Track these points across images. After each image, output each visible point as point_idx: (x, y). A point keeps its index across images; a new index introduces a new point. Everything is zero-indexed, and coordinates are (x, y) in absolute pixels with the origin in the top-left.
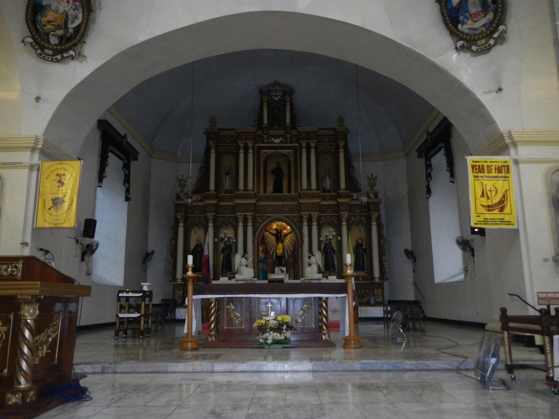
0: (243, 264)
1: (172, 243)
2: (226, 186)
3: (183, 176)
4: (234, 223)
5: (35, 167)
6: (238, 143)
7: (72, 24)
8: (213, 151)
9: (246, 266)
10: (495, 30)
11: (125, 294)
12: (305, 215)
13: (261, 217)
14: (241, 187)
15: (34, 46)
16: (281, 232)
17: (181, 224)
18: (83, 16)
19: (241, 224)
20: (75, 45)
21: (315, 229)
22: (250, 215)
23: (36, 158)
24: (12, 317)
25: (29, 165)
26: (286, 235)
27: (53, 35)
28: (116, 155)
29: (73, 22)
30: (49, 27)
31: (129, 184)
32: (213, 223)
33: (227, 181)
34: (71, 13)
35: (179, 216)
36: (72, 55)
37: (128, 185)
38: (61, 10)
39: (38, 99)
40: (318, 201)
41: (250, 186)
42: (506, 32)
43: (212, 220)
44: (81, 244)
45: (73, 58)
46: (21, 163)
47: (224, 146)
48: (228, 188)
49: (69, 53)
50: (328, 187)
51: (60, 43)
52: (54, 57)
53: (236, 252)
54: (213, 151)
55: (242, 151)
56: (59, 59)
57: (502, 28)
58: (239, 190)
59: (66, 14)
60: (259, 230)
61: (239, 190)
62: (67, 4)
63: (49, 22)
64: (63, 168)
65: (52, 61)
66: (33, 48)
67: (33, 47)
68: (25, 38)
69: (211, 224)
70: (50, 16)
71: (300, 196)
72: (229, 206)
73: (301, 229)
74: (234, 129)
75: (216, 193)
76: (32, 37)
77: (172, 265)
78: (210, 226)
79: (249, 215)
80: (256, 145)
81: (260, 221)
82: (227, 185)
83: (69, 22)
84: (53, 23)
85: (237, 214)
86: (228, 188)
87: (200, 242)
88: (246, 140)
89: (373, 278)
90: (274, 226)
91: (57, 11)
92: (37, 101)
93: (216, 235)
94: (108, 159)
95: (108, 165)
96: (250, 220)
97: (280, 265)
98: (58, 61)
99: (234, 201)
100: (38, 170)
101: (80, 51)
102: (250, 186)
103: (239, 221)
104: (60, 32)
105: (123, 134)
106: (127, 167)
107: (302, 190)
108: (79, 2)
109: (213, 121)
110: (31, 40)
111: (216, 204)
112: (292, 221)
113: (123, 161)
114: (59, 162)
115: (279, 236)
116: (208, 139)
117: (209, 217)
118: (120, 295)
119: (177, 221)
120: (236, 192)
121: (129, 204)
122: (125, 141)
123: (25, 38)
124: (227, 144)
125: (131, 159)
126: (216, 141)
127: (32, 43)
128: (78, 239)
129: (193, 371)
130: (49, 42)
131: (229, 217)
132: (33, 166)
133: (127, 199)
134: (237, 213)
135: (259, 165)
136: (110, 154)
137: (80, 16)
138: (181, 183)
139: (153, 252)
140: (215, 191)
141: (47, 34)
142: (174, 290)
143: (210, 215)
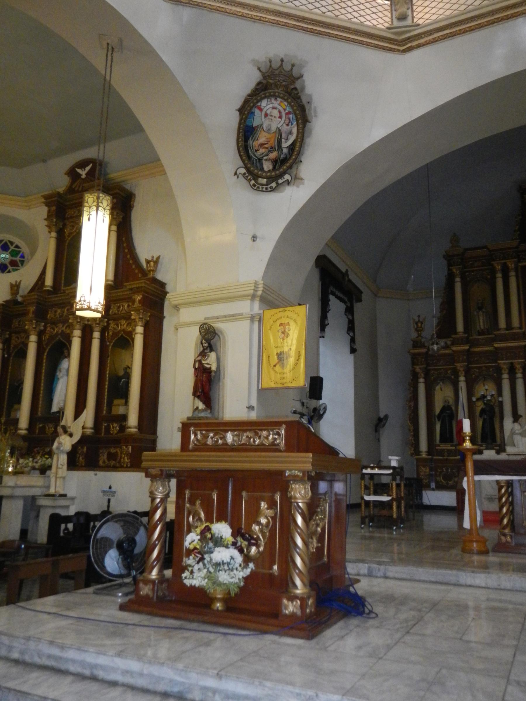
0: (517, 432)
1: (411, 405)
2: (480, 325)
3: (419, 316)
4: (495, 375)
5: (256, 317)
6: (492, 265)
7: (286, 142)
8: (458, 279)
11: (369, 471)
14: (502, 324)
15: (247, 177)
17: (421, 380)
18: (298, 130)
19: (505, 376)
20: (290, 167)
22: (519, 363)
24: (278, 497)
25: (250, 316)
27: (266, 160)
28: (337, 297)
31: (354, 332)
32: (465, 376)
33: (481, 318)
34: (285, 129)
35: (418, 369)
36: (288, 180)
37: (353, 334)
38: (274, 129)
39: (254, 238)
41: (516, 322)
43: (463, 372)
44: (307, 408)
45: (288, 183)
46: (241, 314)
47: (473, 271)
48: (482, 327)
49: (284, 178)
51: (274, 168)
52: (269, 186)
54: (458, 279)
55: (499, 275)
56: (274, 187)
58: (499, 330)
59: (279, 130)
61: (499, 330)
62: (280, 120)
63: (262, 145)
64: (286, 316)
65: (267, 190)
66: (246, 179)
67: (246, 178)
68: (238, 169)
69: (462, 378)
72: (486, 352)
74: (486, 247)
75: (466, 335)
76: (244, 166)
77: (412, 434)
78: (461, 381)
79: (518, 362)
80: (520, 264)
82: (482, 324)
83: (283, 140)
84: (266, 146)
85: (499, 364)
86: (482, 327)
87: (449, 402)
91: (269, 131)
92: (254, 241)
93: (470, 393)
94: (330, 303)
95: (330, 310)
96: (519, 370)
98: (273, 190)
99: (493, 345)
100: (260, 321)
101: (296, 174)
102: (516, 322)
103: (503, 371)
105: (344, 271)
106: (349, 311)
108: (293, 113)
109: (455, 240)
110: (243, 171)
111: (468, 350)
113: (345, 304)
114: (281, 309)
116: (449, 265)
117: (458, 368)
118: (364, 471)
119: (415, 376)
120: (496, 333)
121: (355, 357)
122: (347, 279)
123: (238, 169)
124: (478, 268)
125: (354, 301)
126: (461, 266)
127: (245, 174)
128: (304, 401)
129: (499, 587)
130: (262, 169)
131: (488, 368)
132: (254, 316)
133: (353, 351)
134: (499, 362)
136: (331, 297)
137: (295, 130)
138: (417, 325)
139: (386, 417)
140: (465, 332)
141: (260, 160)
142: (418, 466)
143: (460, 366)
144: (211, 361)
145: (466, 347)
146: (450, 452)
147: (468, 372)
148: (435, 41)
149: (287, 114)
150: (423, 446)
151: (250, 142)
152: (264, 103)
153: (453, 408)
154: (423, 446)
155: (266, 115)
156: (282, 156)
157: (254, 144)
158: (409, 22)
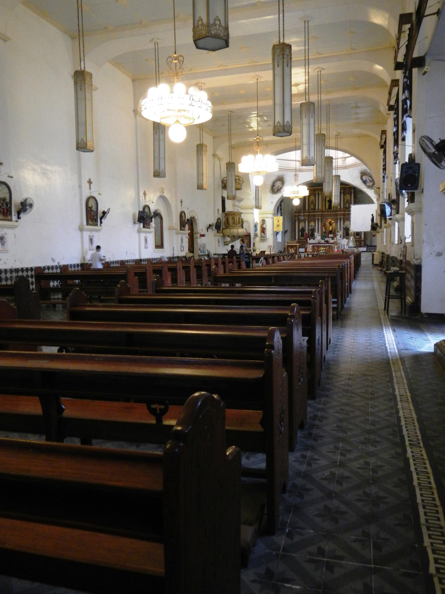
9: (319, 236)
10: (374, 186)
12: (339, 217)
13: (323, 218)
16: (331, 222)
19: (317, 221)
21: (342, 222)
23: (272, 216)
26: (333, 223)
32: (308, 221)
35: (296, 219)
38: (278, 185)
39: (272, 202)
40: (343, 212)
41: (320, 208)
50: (348, 207)
53: (315, 231)
59: (279, 186)
60: (323, 223)
70: (276, 186)
71: (337, 211)
72: (312, 215)
73: (337, 222)
79: (320, 218)
81: (323, 219)
88: (318, 191)
89: (361, 238)
90: (329, 220)
97: (331, 233)
104: (277, 189)
107: (338, 209)
110: (271, 191)
112: (335, 219)
115: (331, 224)
135: (323, 200)
141: (275, 190)
143: (307, 218)
144: (264, 226)
145: (308, 214)
146: (303, 239)
147: (308, 220)
148: (307, 171)
150: (297, 238)
151: (274, 187)
153: (304, 228)
154: (297, 238)
157: (274, 187)
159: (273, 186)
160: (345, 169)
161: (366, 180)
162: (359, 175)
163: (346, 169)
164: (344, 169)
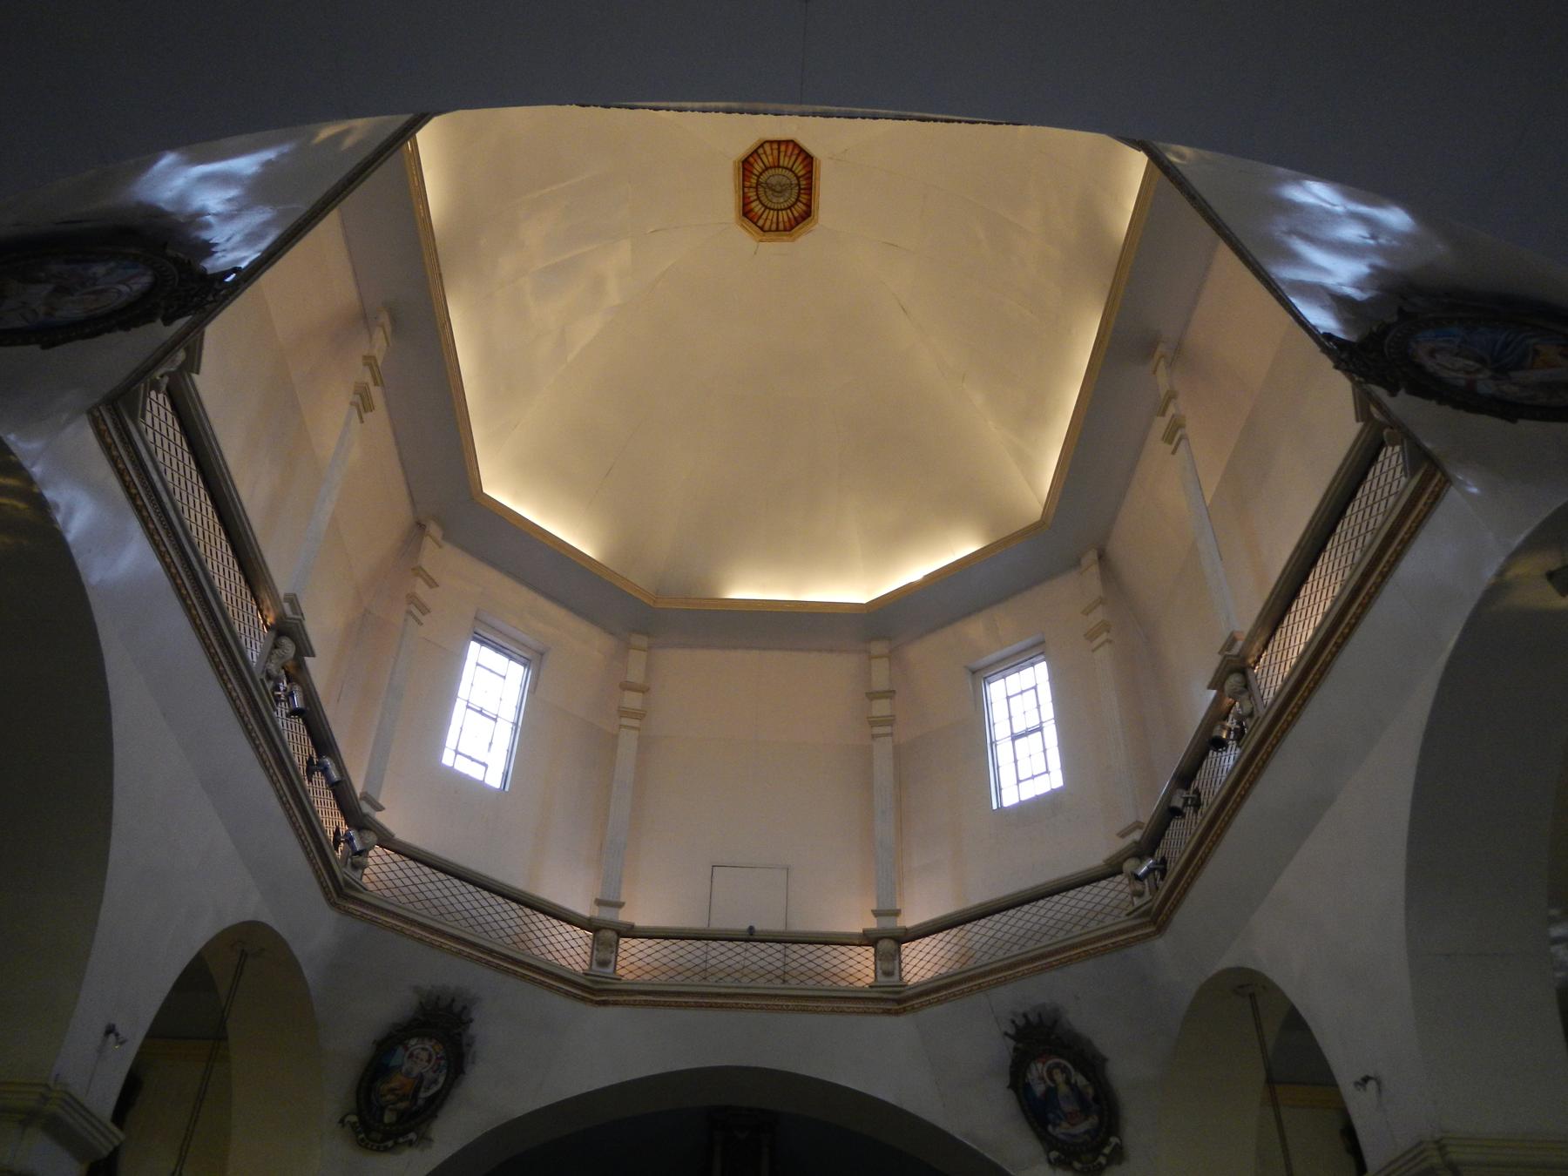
7: (425, 1092)
10: (1105, 1143)
18: (446, 1080)
27: (391, 1110)
29: (428, 1088)
30: (390, 1097)
38: (415, 1073)
42: (1121, 1148)
45: (410, 1143)
52: (382, 1145)
57: (1114, 1140)
59: (421, 1077)
62: (426, 1064)
63: (392, 1091)
65: (378, 1150)
83: (423, 1089)
84: (397, 1092)
91: (408, 1074)
98: (386, 1149)
104: (402, 1105)
110: (354, 1118)
137: (441, 1080)
141: (383, 1109)
148: (634, 1004)
149: (437, 1058)
152: (413, 1042)
155: (411, 1056)
156: (414, 1108)
158: (610, 970)
159: (377, 1068)
160: (897, 1013)
161: (1051, 1092)
162: (1000, 1050)
163: (905, 1010)
164: (888, 1012)
